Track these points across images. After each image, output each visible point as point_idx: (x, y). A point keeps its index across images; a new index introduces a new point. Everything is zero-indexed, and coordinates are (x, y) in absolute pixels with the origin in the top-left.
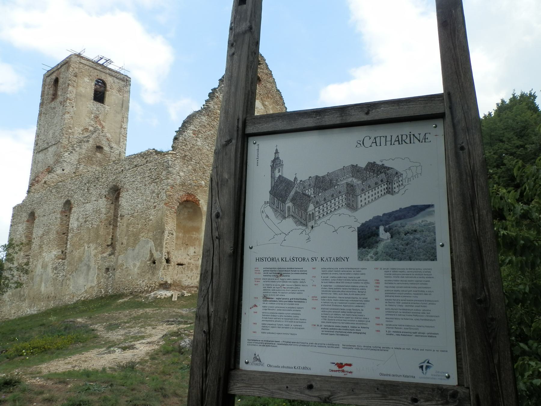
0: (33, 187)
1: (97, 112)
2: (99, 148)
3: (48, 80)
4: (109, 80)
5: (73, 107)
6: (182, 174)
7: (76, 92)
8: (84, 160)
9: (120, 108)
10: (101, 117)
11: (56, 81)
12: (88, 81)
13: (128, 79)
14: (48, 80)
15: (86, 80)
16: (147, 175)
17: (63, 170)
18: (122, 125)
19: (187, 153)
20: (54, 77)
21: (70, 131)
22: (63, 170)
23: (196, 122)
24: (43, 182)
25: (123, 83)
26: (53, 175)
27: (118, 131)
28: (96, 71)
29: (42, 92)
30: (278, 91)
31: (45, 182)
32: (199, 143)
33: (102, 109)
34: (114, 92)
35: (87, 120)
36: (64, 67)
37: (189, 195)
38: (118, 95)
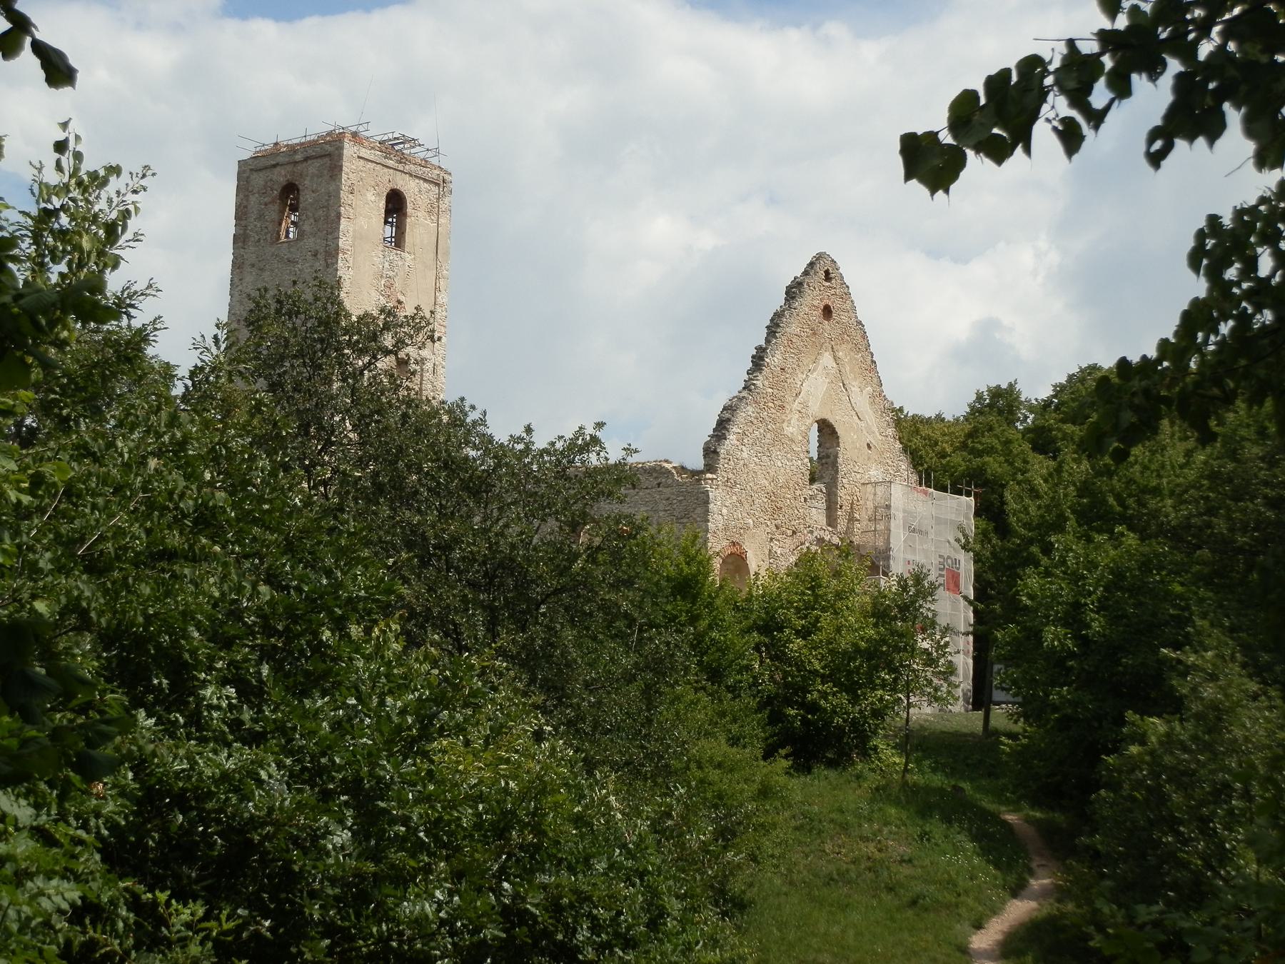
1: (391, 274)
3: (258, 180)
4: (410, 188)
6: (725, 511)
7: (354, 231)
11: (289, 194)
12: (373, 198)
13: (446, 177)
14: (258, 180)
15: (370, 196)
16: (661, 507)
19: (731, 476)
20: (280, 176)
23: (741, 417)
28: (386, 170)
29: (238, 207)
30: (860, 323)
32: (745, 455)
33: (400, 263)
34: (421, 214)
36: (317, 163)
37: (734, 544)
38: (428, 222)
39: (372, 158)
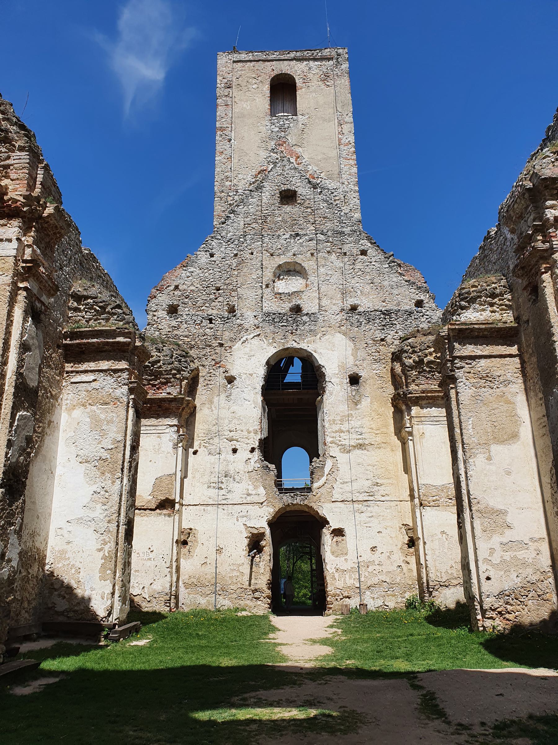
0: (154, 300)
2: (288, 197)
5: (230, 140)
8: (254, 225)
9: (331, 111)
10: (292, 139)
17: (212, 255)
18: (340, 140)
21: (228, 183)
22: (212, 255)
24: (172, 288)
25: (331, 62)
26: (192, 269)
27: (334, 153)
31: (177, 287)
34: (315, 83)
35: (263, 154)
38: (323, 86)
39: (251, 58)
